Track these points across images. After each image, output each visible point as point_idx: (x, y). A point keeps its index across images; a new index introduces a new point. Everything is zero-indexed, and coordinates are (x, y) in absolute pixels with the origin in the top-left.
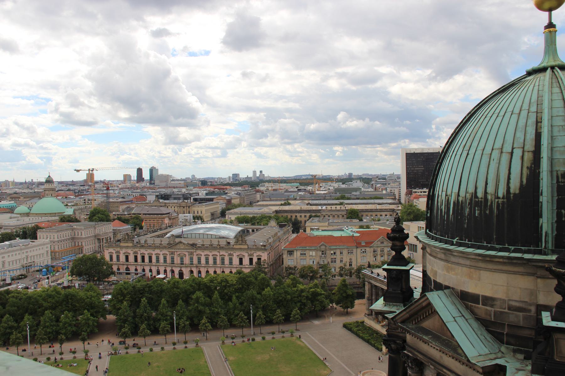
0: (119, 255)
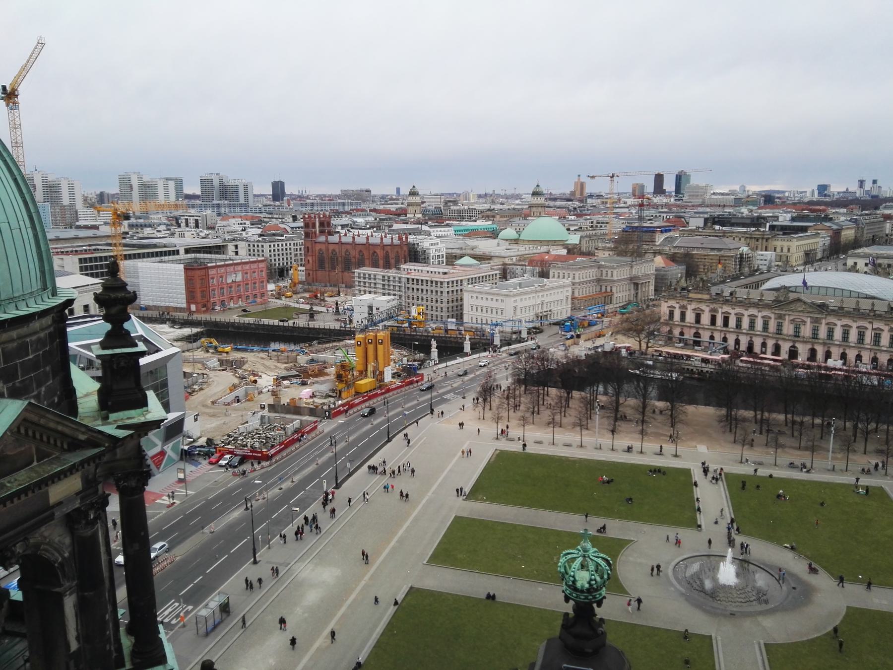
0: (685, 312)
